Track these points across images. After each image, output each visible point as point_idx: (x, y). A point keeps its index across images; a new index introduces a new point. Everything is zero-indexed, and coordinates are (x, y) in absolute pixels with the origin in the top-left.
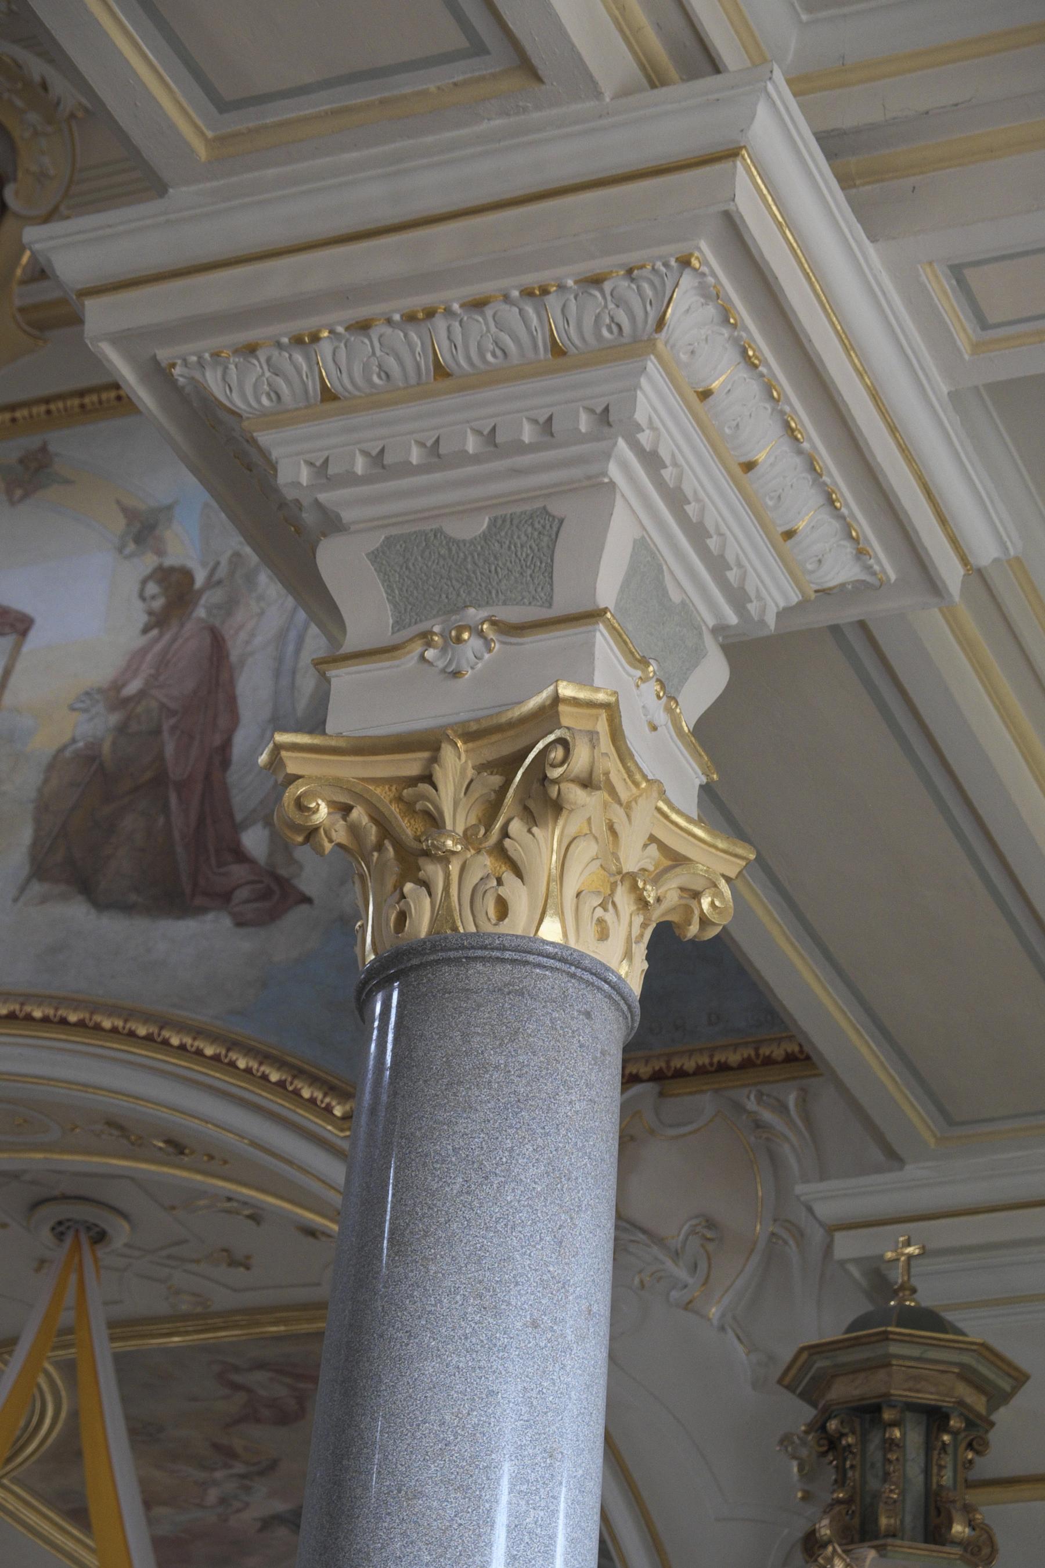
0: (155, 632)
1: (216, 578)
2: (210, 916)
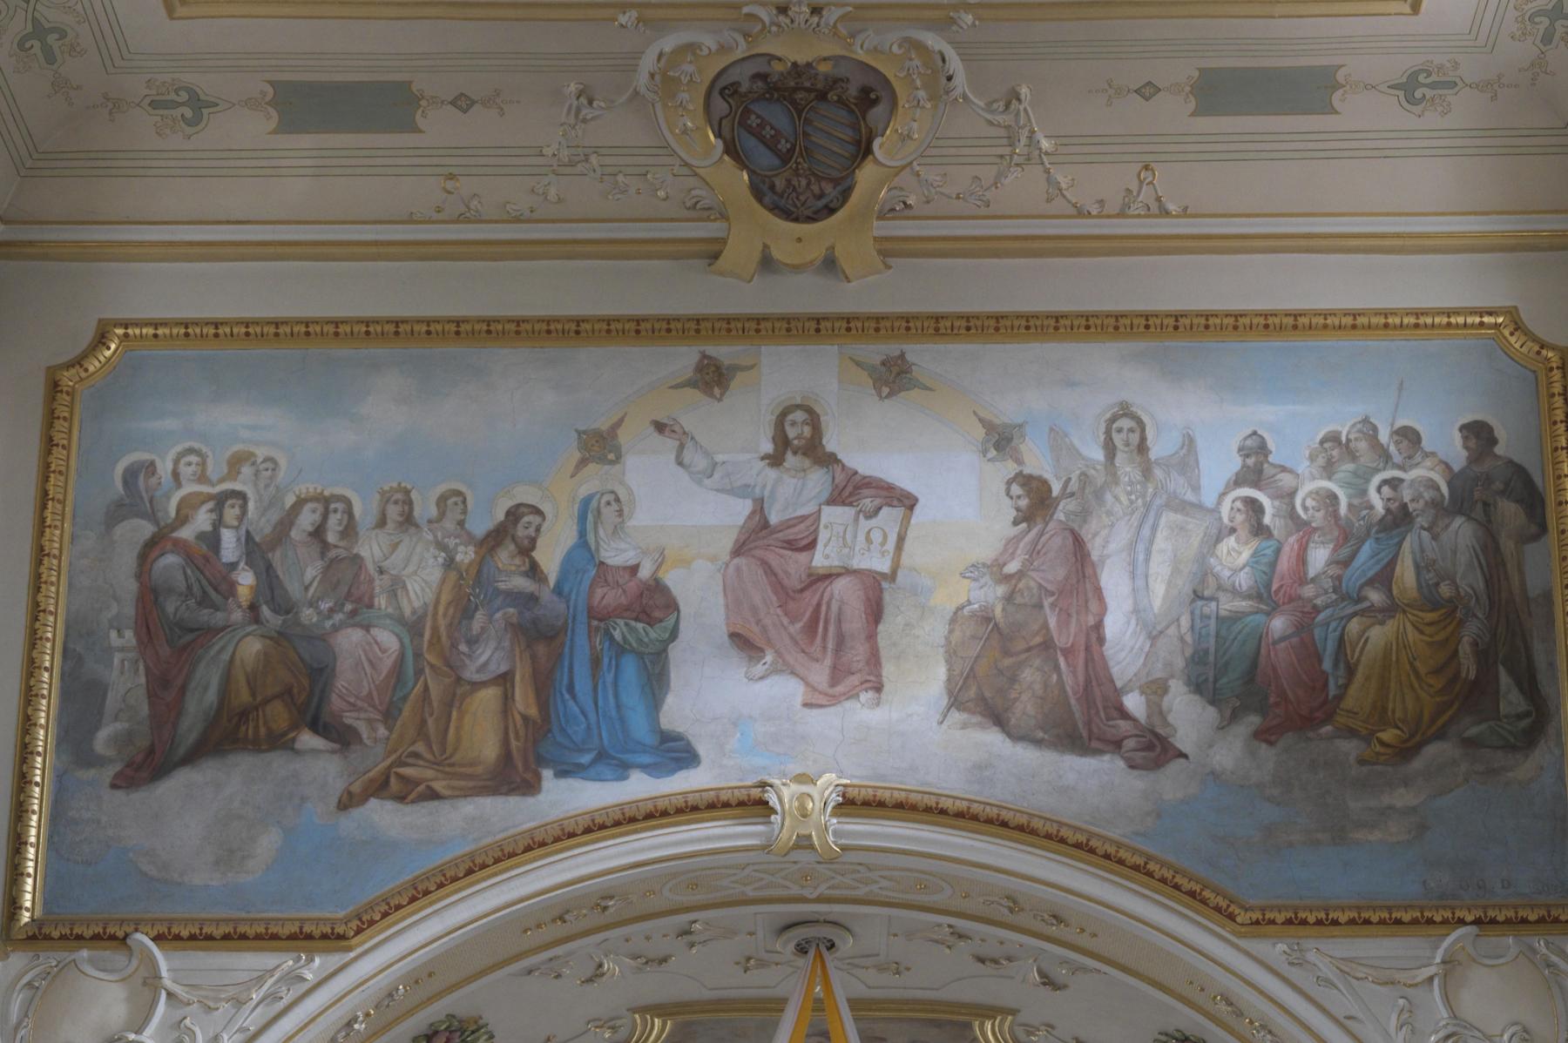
0: (1024, 525)
1: (1068, 491)
2: (1107, 757)
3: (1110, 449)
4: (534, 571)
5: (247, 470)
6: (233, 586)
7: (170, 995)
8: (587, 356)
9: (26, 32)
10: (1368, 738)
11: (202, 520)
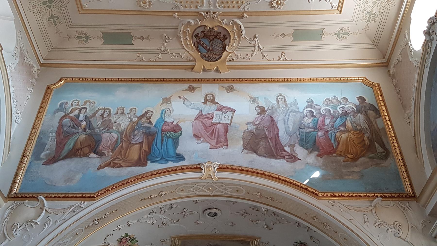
0: (259, 115)
1: (269, 109)
2: (281, 160)
3: (278, 102)
4: (150, 123)
5: (88, 104)
6: (81, 125)
7: (46, 211)
8: (165, 85)
9: (49, 16)
10: (345, 156)
11: (76, 112)
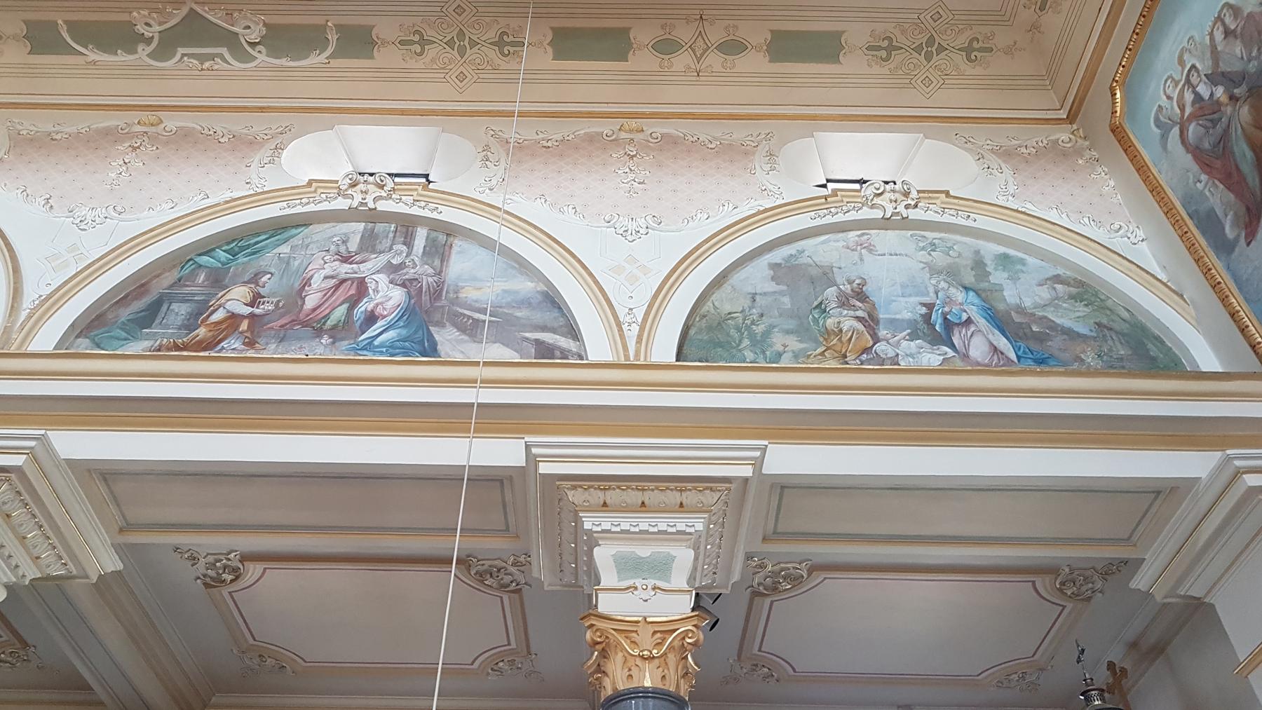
5: (1186, 56)
6: (1218, 103)
9: (964, 56)
11: (1189, 97)
